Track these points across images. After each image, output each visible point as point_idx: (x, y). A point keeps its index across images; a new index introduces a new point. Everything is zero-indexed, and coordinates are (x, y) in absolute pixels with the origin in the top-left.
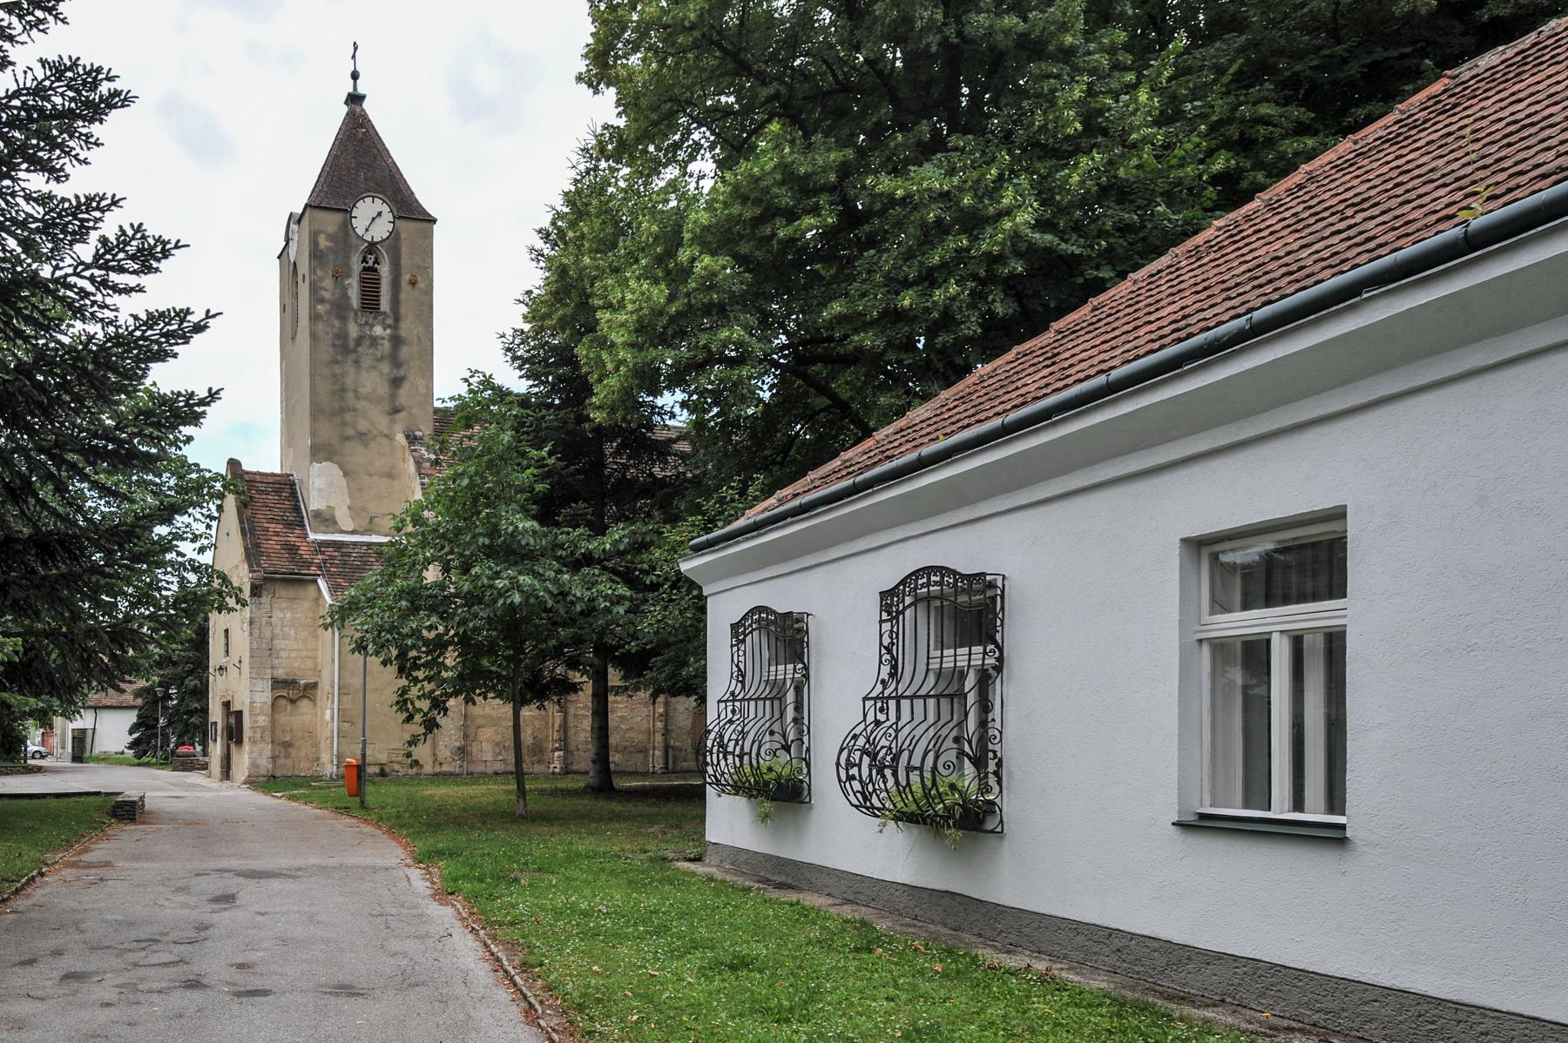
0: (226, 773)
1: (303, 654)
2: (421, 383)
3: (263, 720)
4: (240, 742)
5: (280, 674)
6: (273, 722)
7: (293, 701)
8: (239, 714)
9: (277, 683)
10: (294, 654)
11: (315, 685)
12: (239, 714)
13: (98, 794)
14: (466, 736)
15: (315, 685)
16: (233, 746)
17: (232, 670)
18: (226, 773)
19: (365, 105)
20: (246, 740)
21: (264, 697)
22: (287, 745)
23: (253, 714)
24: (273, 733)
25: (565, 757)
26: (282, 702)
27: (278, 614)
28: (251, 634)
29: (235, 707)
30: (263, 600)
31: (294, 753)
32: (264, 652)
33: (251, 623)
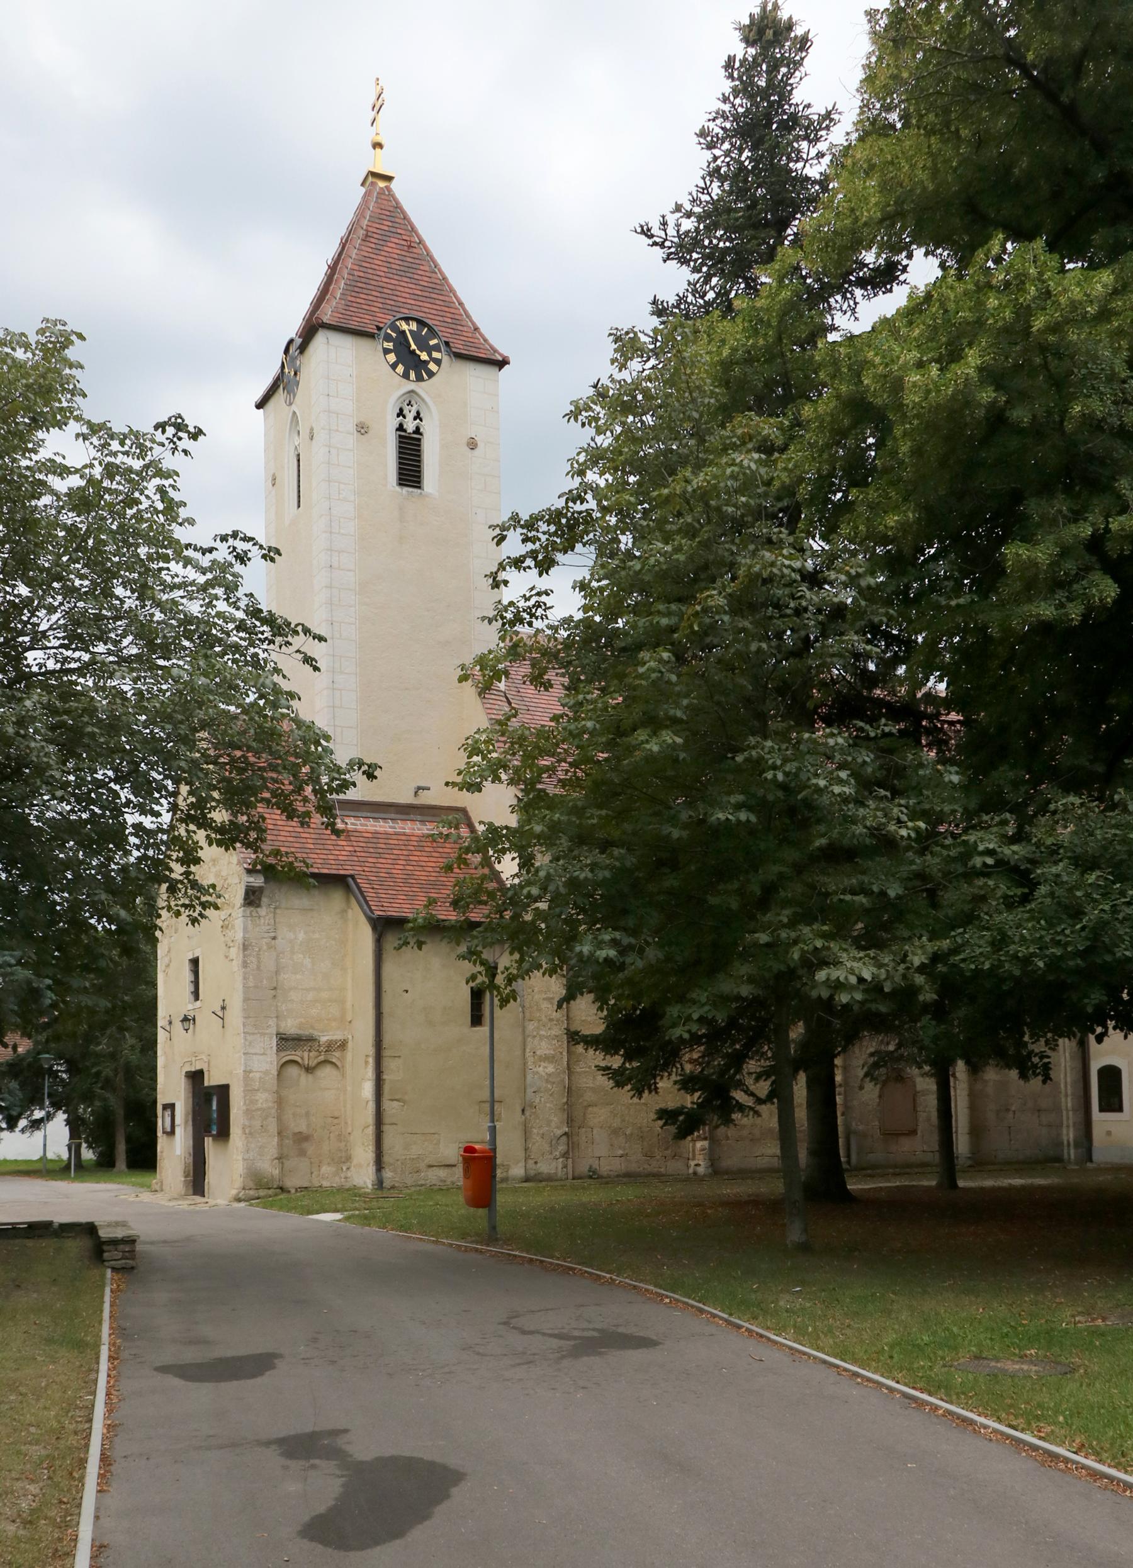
0: (197, 1180)
1: (325, 995)
2: (148, 949)
3: (264, 1099)
4: (224, 1134)
5: (291, 1027)
6: (280, 1102)
7: (309, 1070)
8: (223, 1091)
9: (285, 1041)
10: (310, 996)
11: (343, 1045)
12: (223, 1091)
13: (333, 269)
14: (570, 1121)
15: (343, 1045)
16: (208, 1142)
17: (206, 1022)
18: (197, 1180)
19: (393, 185)
20: (235, 1130)
21: (266, 1061)
22: (302, 1138)
23: (249, 1090)
24: (279, 1119)
25: (711, 1149)
26: (293, 1071)
27: (284, 934)
28: (245, 964)
29: (212, 1079)
30: (263, 911)
31: (311, 1149)
32: (265, 991)
33: (245, 947)
